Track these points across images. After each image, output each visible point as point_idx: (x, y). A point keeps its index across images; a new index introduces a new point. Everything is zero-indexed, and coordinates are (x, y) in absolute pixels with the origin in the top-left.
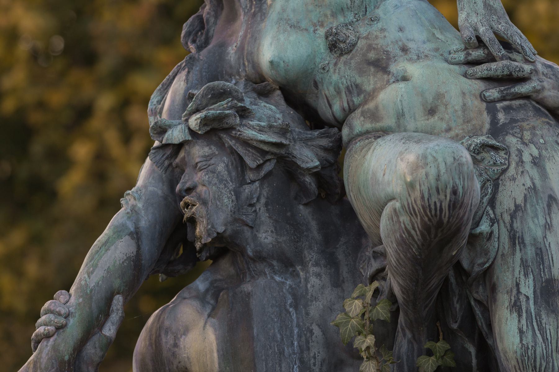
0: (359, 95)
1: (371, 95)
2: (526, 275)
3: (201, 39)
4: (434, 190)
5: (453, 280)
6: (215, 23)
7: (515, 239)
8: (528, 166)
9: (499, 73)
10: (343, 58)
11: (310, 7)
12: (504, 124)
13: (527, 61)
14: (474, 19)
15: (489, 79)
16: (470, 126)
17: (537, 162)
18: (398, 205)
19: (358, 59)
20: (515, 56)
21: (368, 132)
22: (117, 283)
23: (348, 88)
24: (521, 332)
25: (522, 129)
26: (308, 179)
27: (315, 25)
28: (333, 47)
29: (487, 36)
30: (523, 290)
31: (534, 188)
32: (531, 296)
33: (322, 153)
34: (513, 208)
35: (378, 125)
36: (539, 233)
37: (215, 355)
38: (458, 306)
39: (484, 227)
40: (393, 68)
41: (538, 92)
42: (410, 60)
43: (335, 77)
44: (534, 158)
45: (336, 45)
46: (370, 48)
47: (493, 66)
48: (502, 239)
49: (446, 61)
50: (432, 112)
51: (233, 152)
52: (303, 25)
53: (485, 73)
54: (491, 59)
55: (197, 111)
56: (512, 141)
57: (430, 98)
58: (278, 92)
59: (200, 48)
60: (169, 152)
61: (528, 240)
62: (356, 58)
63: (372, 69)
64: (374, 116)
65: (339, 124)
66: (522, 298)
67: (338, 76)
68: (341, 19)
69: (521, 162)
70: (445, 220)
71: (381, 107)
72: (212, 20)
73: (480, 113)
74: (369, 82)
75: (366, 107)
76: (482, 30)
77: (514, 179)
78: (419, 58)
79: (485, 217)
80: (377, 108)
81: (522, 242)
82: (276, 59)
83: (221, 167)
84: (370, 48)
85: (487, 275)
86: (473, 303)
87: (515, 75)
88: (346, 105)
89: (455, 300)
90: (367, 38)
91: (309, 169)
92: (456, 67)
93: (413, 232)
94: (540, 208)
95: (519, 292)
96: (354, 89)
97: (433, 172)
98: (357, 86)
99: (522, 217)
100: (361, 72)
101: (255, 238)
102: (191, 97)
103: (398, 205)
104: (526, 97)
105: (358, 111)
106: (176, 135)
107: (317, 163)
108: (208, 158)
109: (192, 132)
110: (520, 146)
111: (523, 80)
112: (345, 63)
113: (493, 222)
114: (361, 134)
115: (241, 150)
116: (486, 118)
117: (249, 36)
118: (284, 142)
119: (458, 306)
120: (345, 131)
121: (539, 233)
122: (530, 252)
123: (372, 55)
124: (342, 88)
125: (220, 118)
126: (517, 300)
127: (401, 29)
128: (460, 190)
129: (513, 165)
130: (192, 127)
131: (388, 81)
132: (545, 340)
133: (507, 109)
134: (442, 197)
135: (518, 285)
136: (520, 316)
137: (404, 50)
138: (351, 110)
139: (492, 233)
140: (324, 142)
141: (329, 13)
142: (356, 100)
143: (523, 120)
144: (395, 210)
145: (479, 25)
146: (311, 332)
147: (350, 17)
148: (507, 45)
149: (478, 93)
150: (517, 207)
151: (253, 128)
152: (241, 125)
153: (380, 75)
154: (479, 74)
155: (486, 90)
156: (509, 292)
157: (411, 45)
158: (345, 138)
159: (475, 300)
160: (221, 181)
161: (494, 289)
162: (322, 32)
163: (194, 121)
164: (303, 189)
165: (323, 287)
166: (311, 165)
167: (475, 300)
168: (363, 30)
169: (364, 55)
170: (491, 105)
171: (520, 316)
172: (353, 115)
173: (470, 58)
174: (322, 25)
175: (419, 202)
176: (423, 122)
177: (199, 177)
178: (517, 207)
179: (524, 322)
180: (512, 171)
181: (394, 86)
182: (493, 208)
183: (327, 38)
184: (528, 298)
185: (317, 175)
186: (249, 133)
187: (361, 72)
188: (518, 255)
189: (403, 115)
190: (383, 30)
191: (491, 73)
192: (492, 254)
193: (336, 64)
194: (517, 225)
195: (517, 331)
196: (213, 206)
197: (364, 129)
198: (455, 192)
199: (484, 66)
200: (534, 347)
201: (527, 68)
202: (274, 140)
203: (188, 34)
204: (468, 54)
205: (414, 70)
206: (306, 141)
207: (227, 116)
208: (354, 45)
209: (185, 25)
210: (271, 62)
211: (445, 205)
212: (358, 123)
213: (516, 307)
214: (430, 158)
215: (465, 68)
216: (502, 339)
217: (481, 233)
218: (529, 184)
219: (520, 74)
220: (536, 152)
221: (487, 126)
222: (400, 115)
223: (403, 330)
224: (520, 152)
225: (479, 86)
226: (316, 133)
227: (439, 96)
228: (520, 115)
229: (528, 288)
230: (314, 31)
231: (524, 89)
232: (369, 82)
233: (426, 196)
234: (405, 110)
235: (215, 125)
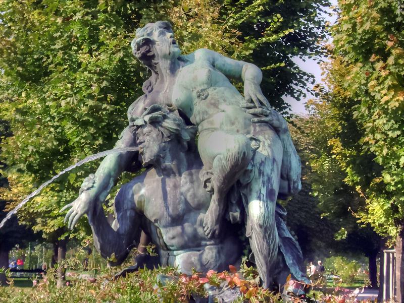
0: (206, 115)
1: (211, 116)
2: (264, 186)
3: (150, 88)
5: (235, 186)
6: (155, 84)
7: (261, 173)
8: (267, 147)
13: (268, 109)
15: (255, 115)
18: (222, 157)
20: (264, 107)
21: (209, 129)
22: (112, 173)
26: (185, 143)
27: (193, 88)
29: (254, 99)
33: (191, 135)
34: (260, 162)
35: (213, 127)
36: (269, 173)
39: (250, 168)
42: (227, 104)
50: (233, 124)
55: (148, 114)
56: (261, 138)
58: (177, 111)
59: (150, 92)
60: (135, 127)
61: (265, 174)
63: (212, 106)
64: (212, 123)
65: (198, 124)
66: (262, 196)
67: (199, 107)
69: (264, 145)
70: (239, 164)
72: (154, 83)
74: (211, 111)
78: (230, 104)
79: (250, 164)
81: (263, 175)
83: (154, 136)
84: (212, 99)
85: (248, 186)
86: (242, 194)
88: (201, 118)
91: (186, 140)
93: (227, 167)
98: (206, 112)
100: (208, 107)
102: (145, 109)
103: (222, 157)
106: (139, 122)
107: (189, 138)
108: (150, 131)
109: (145, 122)
110: (264, 140)
114: (205, 129)
117: (168, 90)
118: (179, 128)
122: (266, 178)
123: (213, 101)
125: (156, 118)
126: (260, 195)
128: (246, 154)
130: (145, 120)
131: (218, 112)
132: (268, 211)
134: (240, 155)
135: (260, 190)
142: (205, 117)
143: (265, 130)
144: (221, 159)
146: (181, 199)
148: (261, 103)
150: (262, 162)
156: (257, 192)
158: (199, 130)
159: (243, 194)
161: (251, 190)
163: (147, 118)
164: (183, 146)
165: (186, 183)
166: (187, 138)
167: (243, 194)
169: (210, 101)
172: (204, 122)
175: (231, 157)
176: (229, 127)
177: (147, 138)
178: (262, 162)
182: (253, 161)
185: (188, 143)
187: (208, 107)
188: (261, 179)
189: (223, 124)
191: (255, 112)
192: (251, 177)
193: (199, 103)
194: (262, 168)
196: (150, 147)
197: (207, 128)
198: (244, 153)
201: (268, 112)
202: (175, 128)
206: (186, 130)
210: (176, 100)
217: (248, 170)
222: (222, 124)
223: (214, 201)
224: (264, 143)
229: (264, 191)
233: (234, 155)
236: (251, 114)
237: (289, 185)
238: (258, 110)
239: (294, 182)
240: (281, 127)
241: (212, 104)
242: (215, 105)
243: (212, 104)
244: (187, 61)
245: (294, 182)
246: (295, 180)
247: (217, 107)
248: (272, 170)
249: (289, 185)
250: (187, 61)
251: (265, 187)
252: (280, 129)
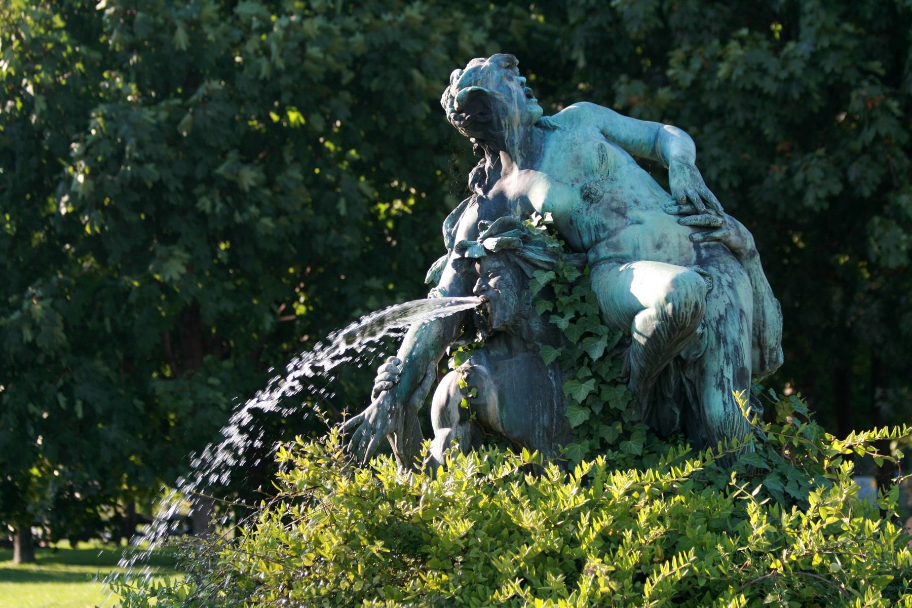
1: (614, 233)
2: (728, 364)
4: (683, 305)
7: (721, 338)
8: (726, 289)
9: (702, 223)
10: (593, 205)
11: (570, 168)
12: (706, 258)
13: (719, 215)
14: (683, 184)
16: (683, 259)
17: (731, 286)
19: (604, 206)
20: (711, 211)
21: (610, 258)
23: (596, 226)
24: (725, 404)
25: (718, 263)
27: (572, 181)
29: (695, 197)
30: (726, 374)
32: (731, 379)
34: (718, 317)
35: (619, 253)
36: (736, 336)
37: (497, 407)
38: (673, 382)
40: (629, 214)
41: (726, 237)
42: (641, 209)
43: (587, 219)
44: (729, 283)
45: (588, 196)
46: (613, 199)
47: (699, 217)
48: (710, 338)
49: (665, 211)
50: (658, 247)
51: (517, 266)
52: (565, 180)
53: (693, 222)
54: (696, 212)
57: (657, 239)
61: (729, 340)
64: (616, 247)
65: (586, 250)
66: (725, 380)
67: (591, 217)
68: (591, 178)
69: (720, 285)
70: (688, 325)
71: (622, 241)
73: (690, 249)
75: (610, 240)
76: (690, 192)
77: (717, 297)
78: (647, 209)
80: (618, 242)
81: (725, 342)
82: (547, 204)
84: (613, 199)
86: (684, 380)
87: (712, 224)
88: (594, 238)
89: (672, 378)
90: (610, 192)
92: (672, 217)
93: (662, 332)
94: (736, 318)
95: (723, 376)
97: (683, 292)
98: (603, 225)
99: (725, 324)
101: (529, 326)
104: (718, 240)
105: (603, 243)
110: (719, 274)
111: (716, 228)
112: (595, 209)
113: (704, 326)
115: (522, 265)
116: (694, 254)
119: (673, 382)
120: (592, 256)
121: (736, 336)
122: (731, 348)
123: (614, 205)
124: (592, 226)
126: (722, 381)
127: (632, 188)
128: (700, 305)
129: (716, 287)
131: (626, 224)
133: (707, 248)
134: (688, 309)
135: (722, 371)
136: (723, 392)
137: (636, 202)
138: (598, 241)
139: (703, 333)
140: (576, 262)
141: (582, 173)
142: (602, 235)
143: (718, 256)
145: (688, 189)
147: (598, 177)
149: (688, 235)
150: (721, 316)
151: (532, 251)
152: (524, 248)
153: (620, 218)
154: (689, 223)
155: (694, 233)
157: (639, 199)
159: (686, 379)
160: (508, 286)
161: (703, 372)
162: (578, 186)
168: (607, 187)
169: (609, 204)
171: (723, 392)
173: (681, 211)
174: (577, 181)
178: (721, 316)
179: (726, 396)
180: (715, 291)
181: (631, 227)
183: (582, 190)
184: (729, 380)
188: (722, 350)
189: (638, 247)
190: (620, 187)
191: (697, 222)
192: (703, 348)
193: (587, 209)
194: (721, 329)
195: (721, 403)
197: (608, 256)
198: (696, 306)
199: (693, 217)
200: (734, 414)
201: (720, 220)
203: (473, 182)
204: (680, 208)
205: (645, 216)
207: (515, 241)
208: (601, 197)
209: (470, 174)
211: (689, 315)
212: (604, 251)
213: (721, 386)
214: (680, 282)
215: (678, 218)
216: (709, 407)
218: (728, 301)
219: (716, 224)
220: (729, 279)
221: (694, 259)
224: (719, 279)
225: (689, 231)
226: (572, 256)
227: (664, 236)
228: (716, 252)
229: (729, 374)
230: (572, 185)
231: (717, 234)
232: (613, 223)
233: (677, 308)
234: (641, 245)
235: (505, 247)
236: (691, 226)
238: (699, 219)
240: (745, 248)
241: (613, 210)
242: (621, 212)
243: (613, 210)
244: (554, 128)
246: (773, 345)
247: (623, 215)
248: (741, 331)
250: (554, 128)
251: (731, 365)
252: (742, 251)
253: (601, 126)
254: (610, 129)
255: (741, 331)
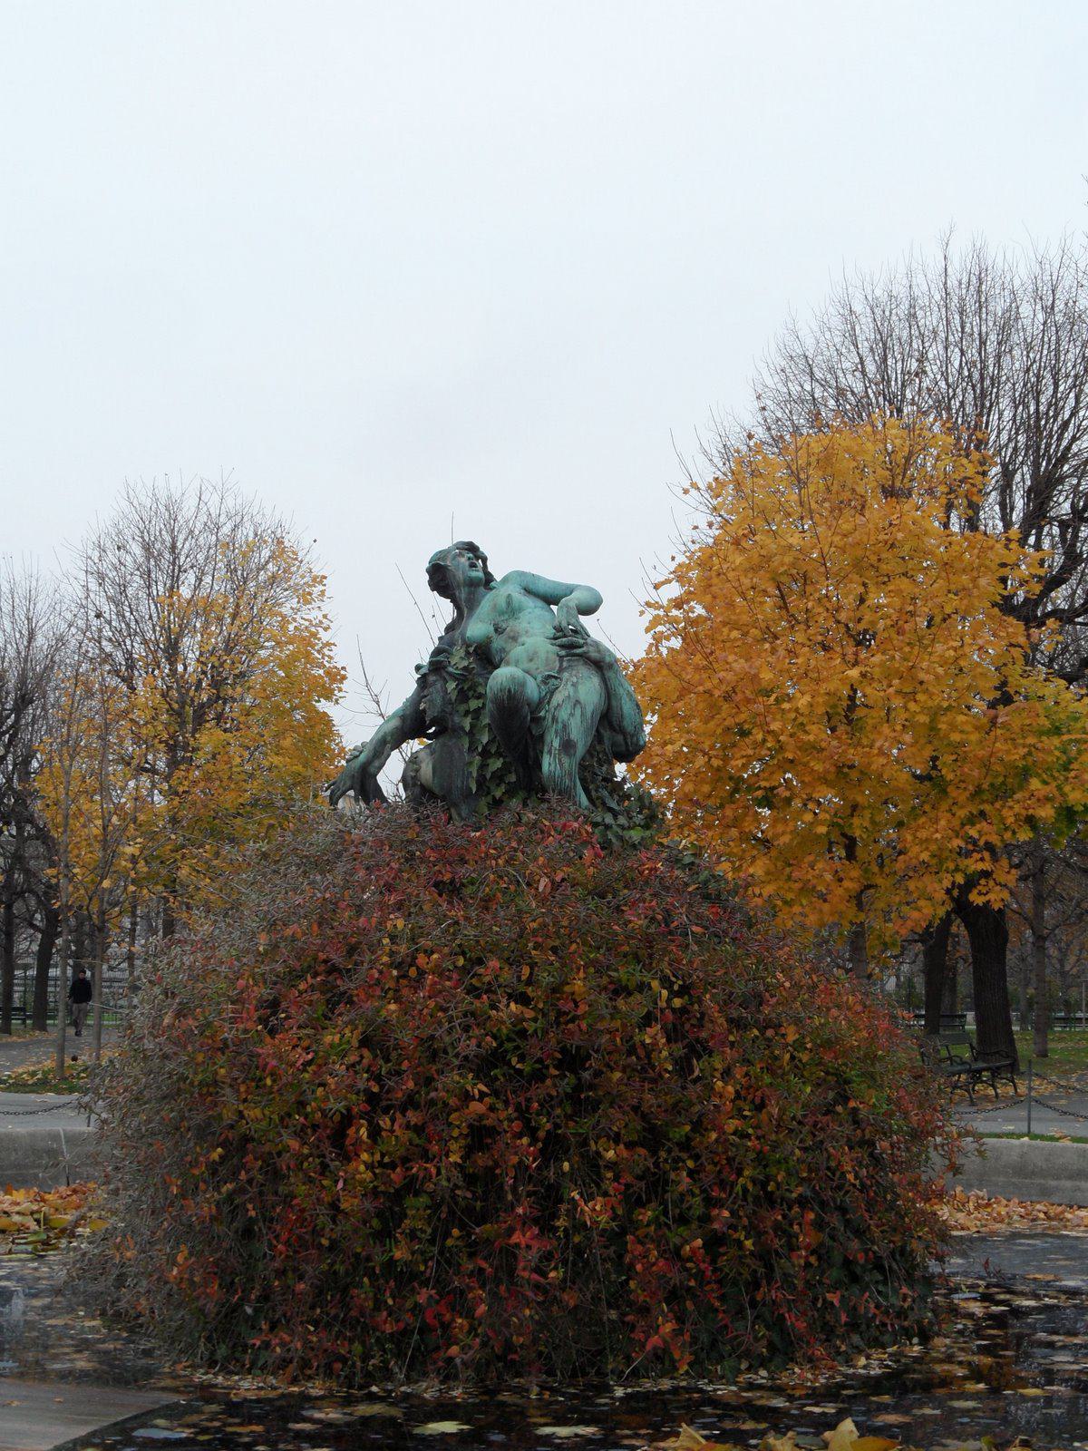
7: (554, 719)
28: (496, 630)
31: (569, 697)
39: (542, 714)
50: (531, 660)
54: (565, 636)
62: (504, 636)
67: (498, 643)
85: (542, 737)
96: (503, 650)
104: (579, 655)
116: (557, 664)
122: (560, 726)
170: (561, 657)
186: (450, 669)
198: (509, 691)
213: (550, 752)
225: (556, 649)
227: (535, 653)
229: (556, 744)
232: (508, 647)
237: (625, 739)
239: (632, 736)
245: (632, 736)
248: (572, 715)
249: (625, 739)
253: (524, 584)
254: (531, 587)
255: (572, 715)
